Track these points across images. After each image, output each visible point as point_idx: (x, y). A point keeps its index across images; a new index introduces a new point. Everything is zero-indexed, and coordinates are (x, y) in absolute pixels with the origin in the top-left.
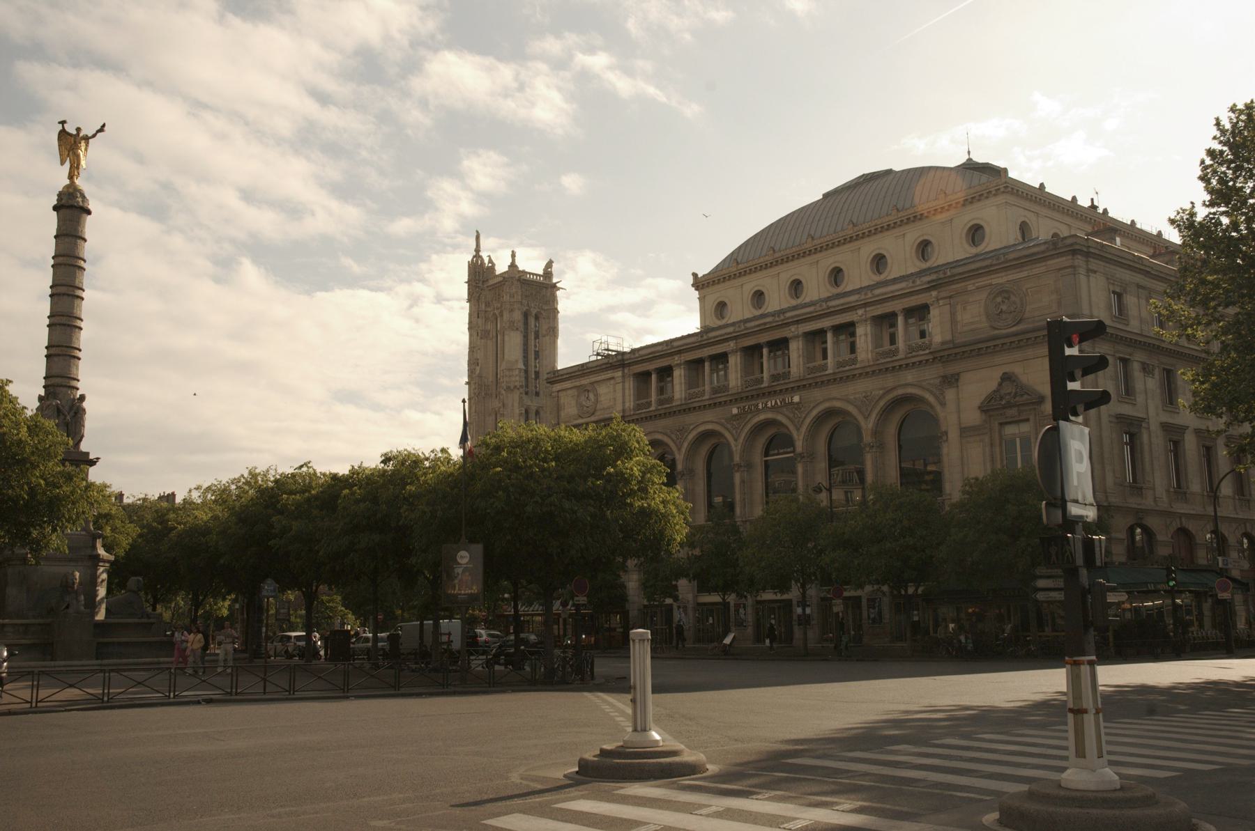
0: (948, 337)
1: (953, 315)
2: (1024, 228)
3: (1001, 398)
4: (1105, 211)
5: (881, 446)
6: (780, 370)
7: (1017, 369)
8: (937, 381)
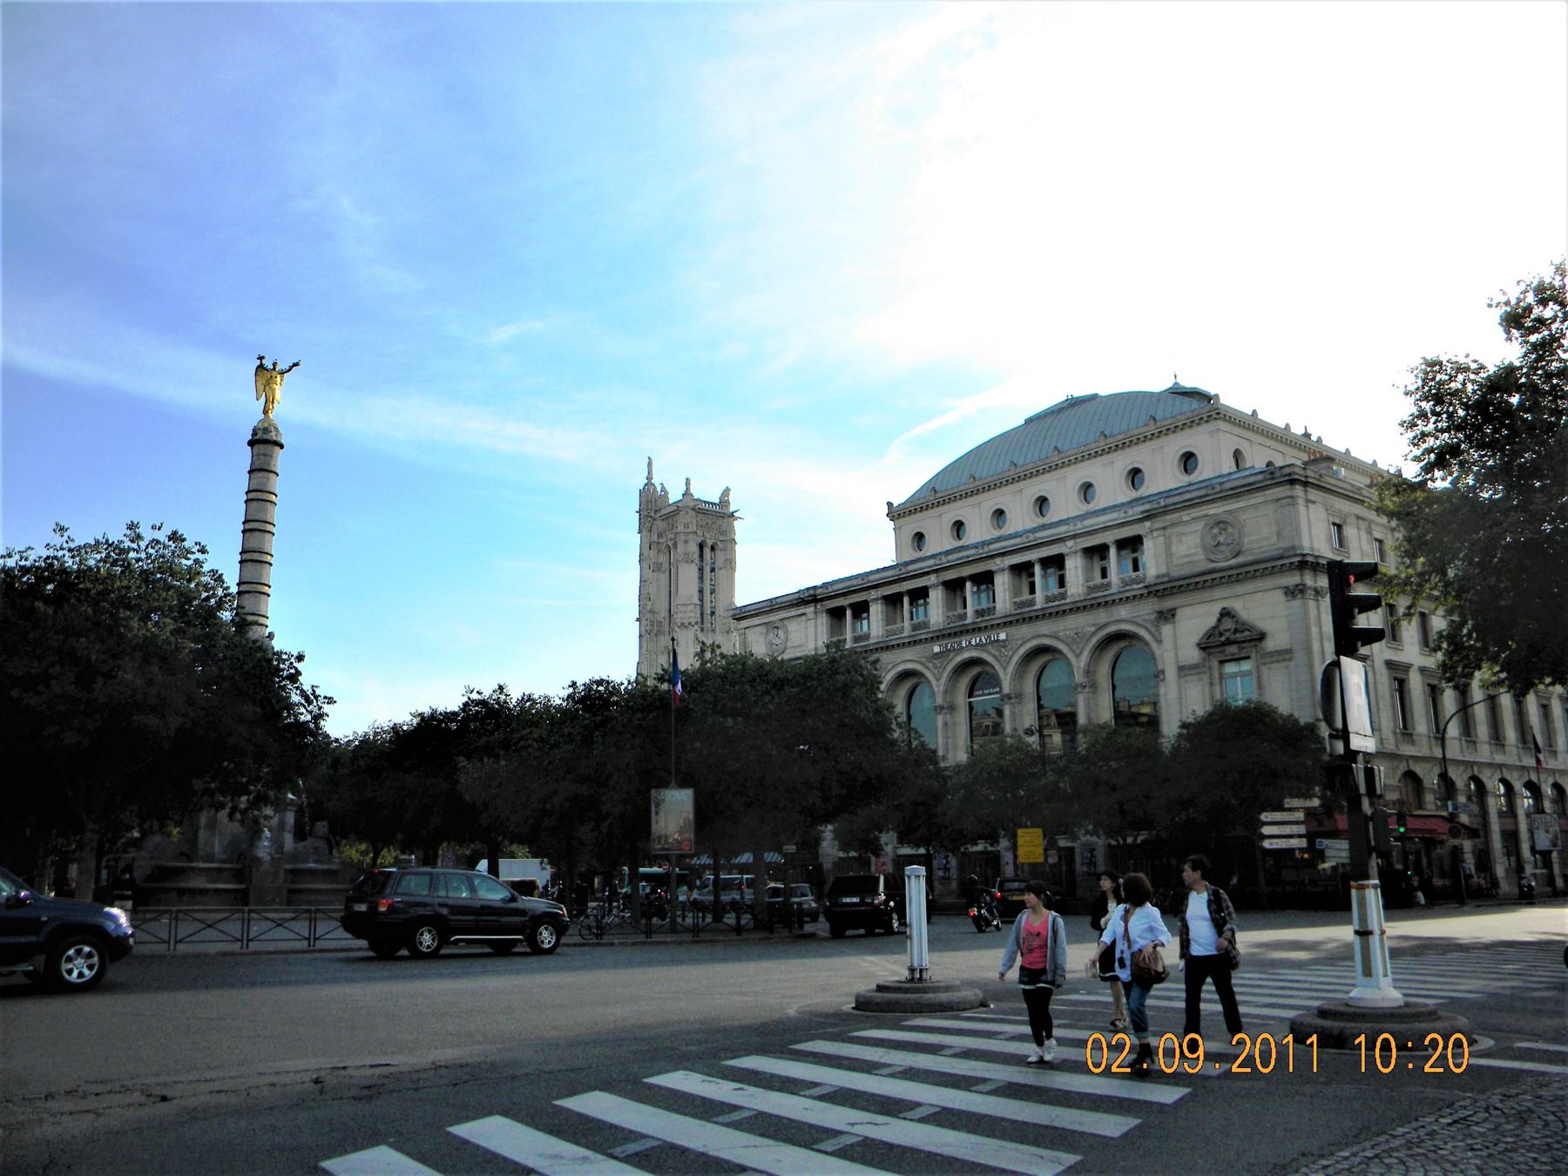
0: (1163, 570)
1: (1168, 545)
2: (1237, 455)
3: (1221, 635)
4: (1319, 440)
5: (1094, 686)
6: (985, 605)
7: (1237, 606)
8: (1153, 617)
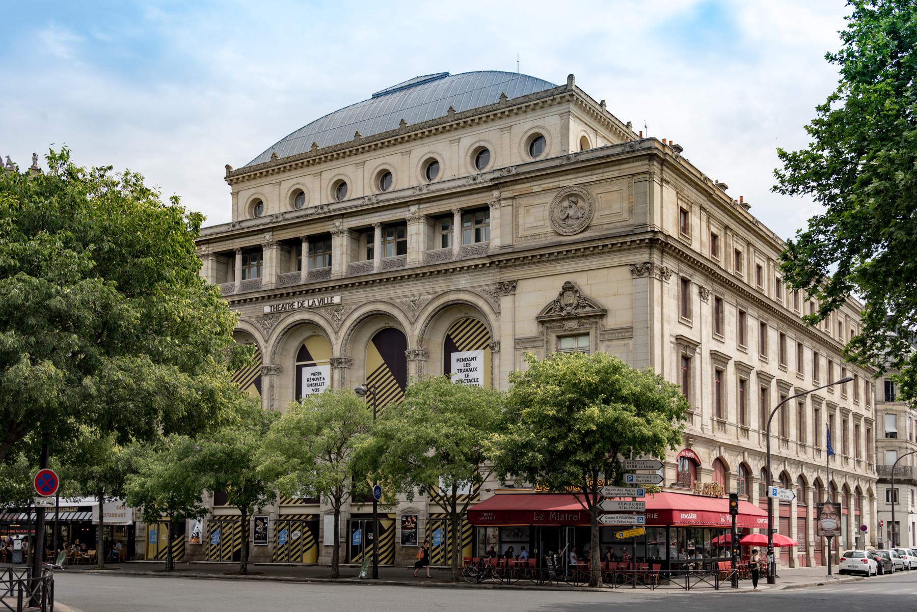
0: (508, 241)
7: (581, 281)
8: (493, 288)
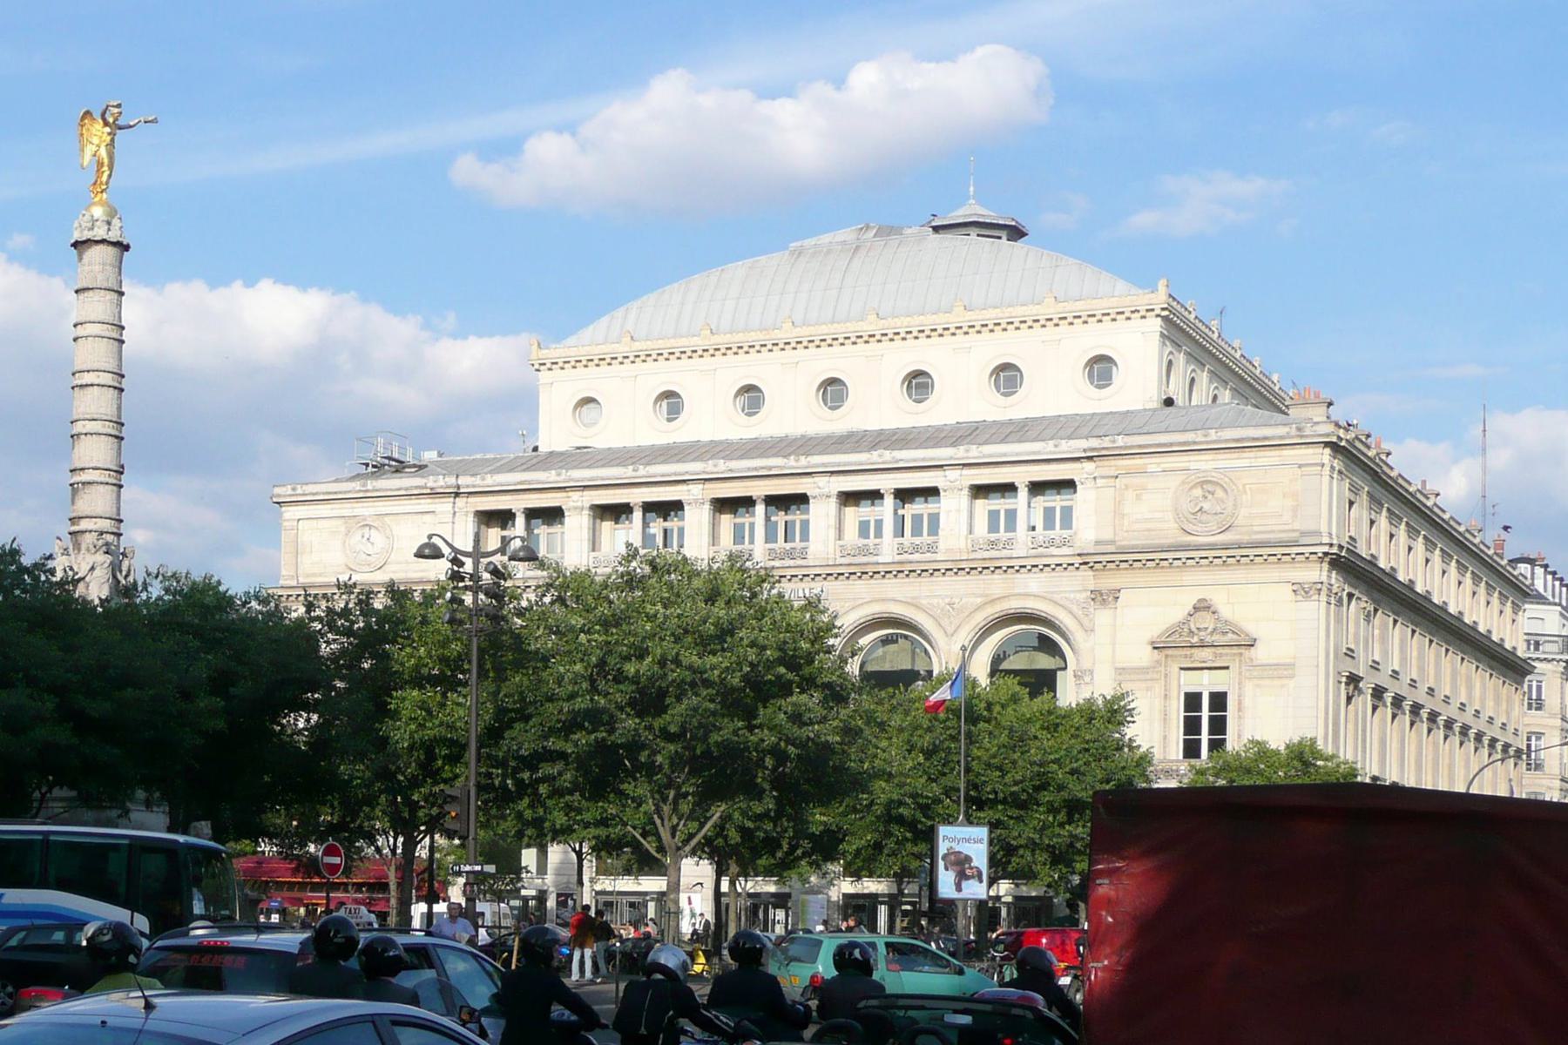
0: (1107, 535)
7: (1218, 598)
